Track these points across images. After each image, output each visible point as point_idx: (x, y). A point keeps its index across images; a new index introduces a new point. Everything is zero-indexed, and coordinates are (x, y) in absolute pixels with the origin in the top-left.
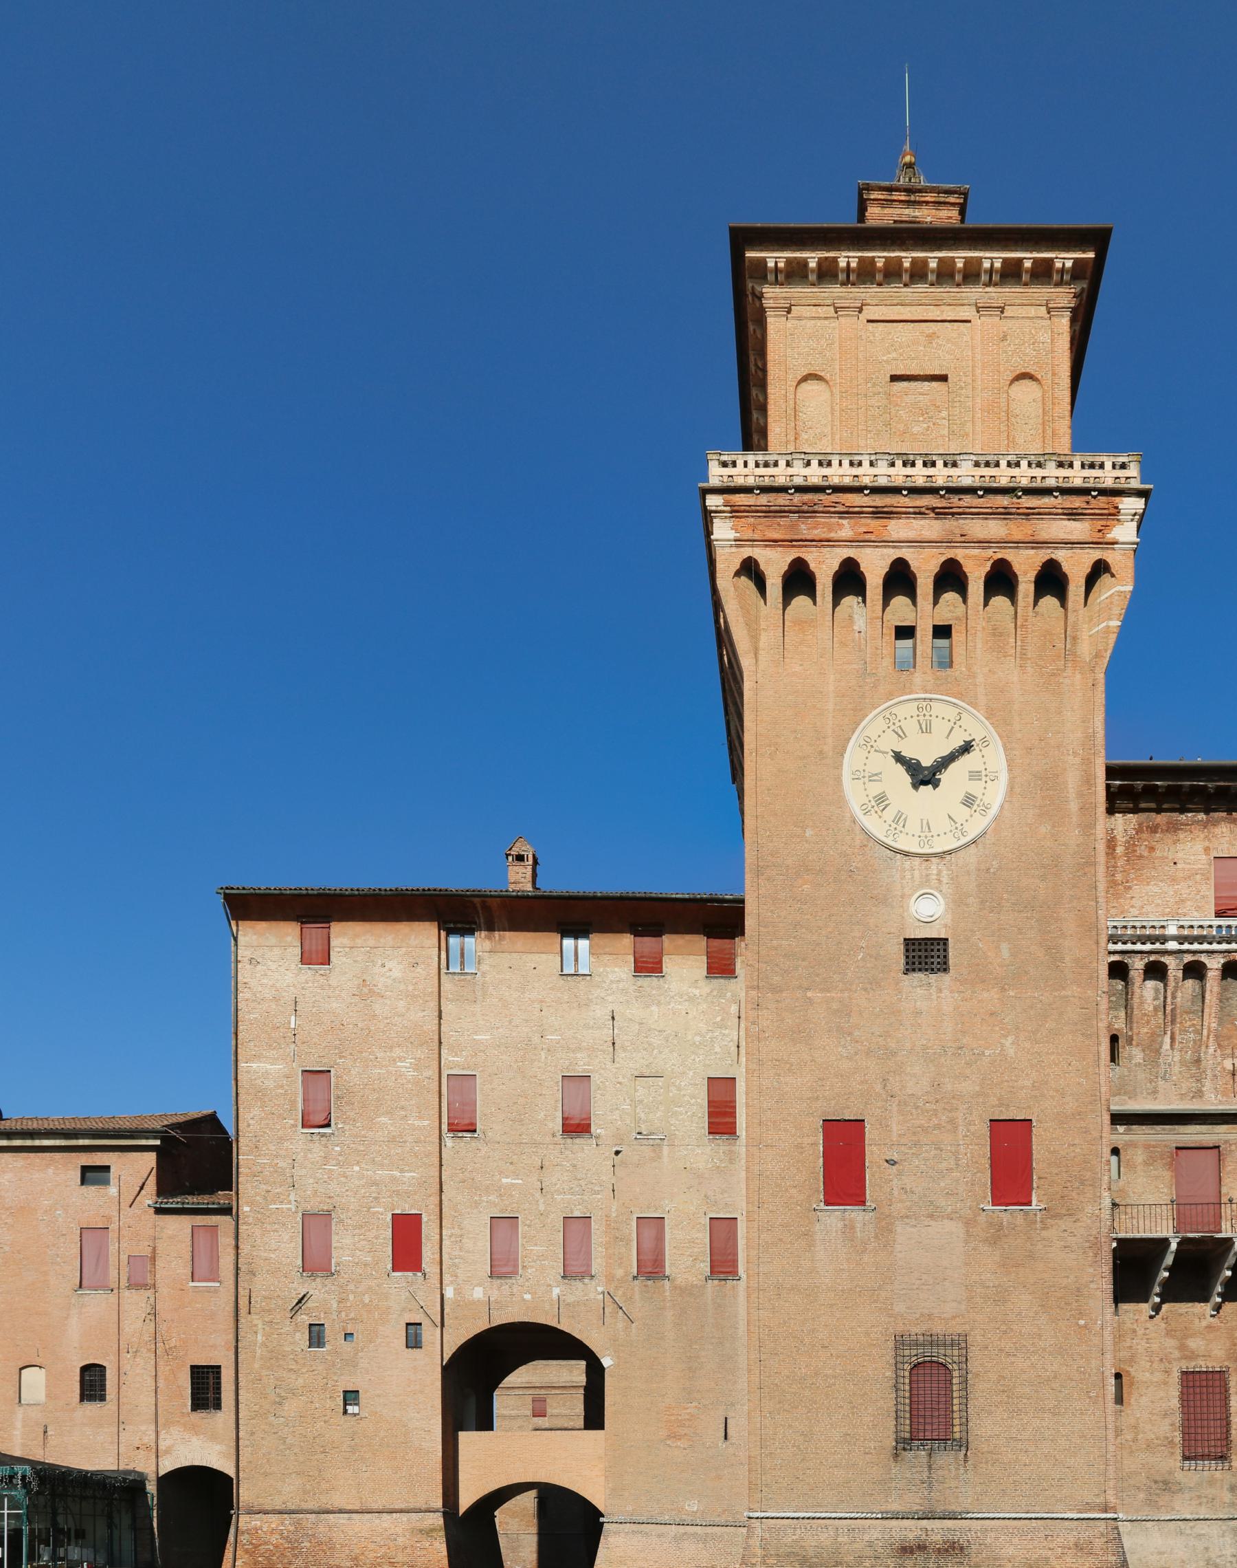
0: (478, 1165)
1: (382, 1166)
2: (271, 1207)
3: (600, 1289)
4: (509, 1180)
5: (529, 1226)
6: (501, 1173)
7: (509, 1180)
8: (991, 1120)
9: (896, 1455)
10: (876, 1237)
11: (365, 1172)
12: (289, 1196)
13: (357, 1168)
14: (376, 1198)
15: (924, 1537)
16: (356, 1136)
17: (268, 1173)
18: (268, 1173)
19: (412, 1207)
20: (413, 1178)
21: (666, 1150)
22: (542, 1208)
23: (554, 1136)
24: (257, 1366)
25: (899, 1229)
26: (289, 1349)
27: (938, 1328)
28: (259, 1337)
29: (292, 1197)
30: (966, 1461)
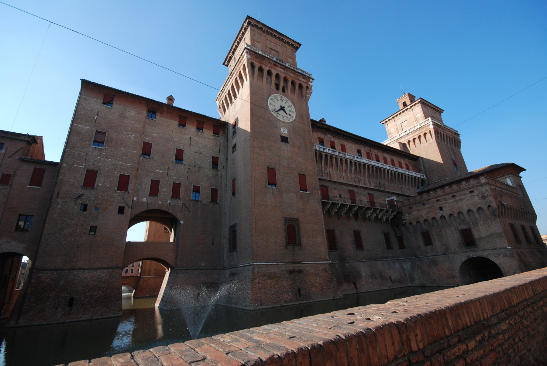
0: (149, 166)
1: (119, 161)
2: (75, 166)
3: (181, 202)
4: (158, 171)
5: (163, 183)
6: (156, 169)
7: (158, 171)
8: (299, 174)
9: (286, 247)
10: (279, 195)
11: (112, 161)
12: (83, 163)
13: (110, 160)
14: (115, 169)
15: (294, 269)
16: (111, 151)
17: (76, 156)
18: (76, 156)
19: (127, 173)
20: (129, 165)
21: (201, 171)
22: (167, 179)
23: (172, 162)
24: (55, 216)
25: (284, 194)
26: (71, 211)
27: (293, 217)
28: (59, 206)
29: (84, 164)
30: (300, 249)
